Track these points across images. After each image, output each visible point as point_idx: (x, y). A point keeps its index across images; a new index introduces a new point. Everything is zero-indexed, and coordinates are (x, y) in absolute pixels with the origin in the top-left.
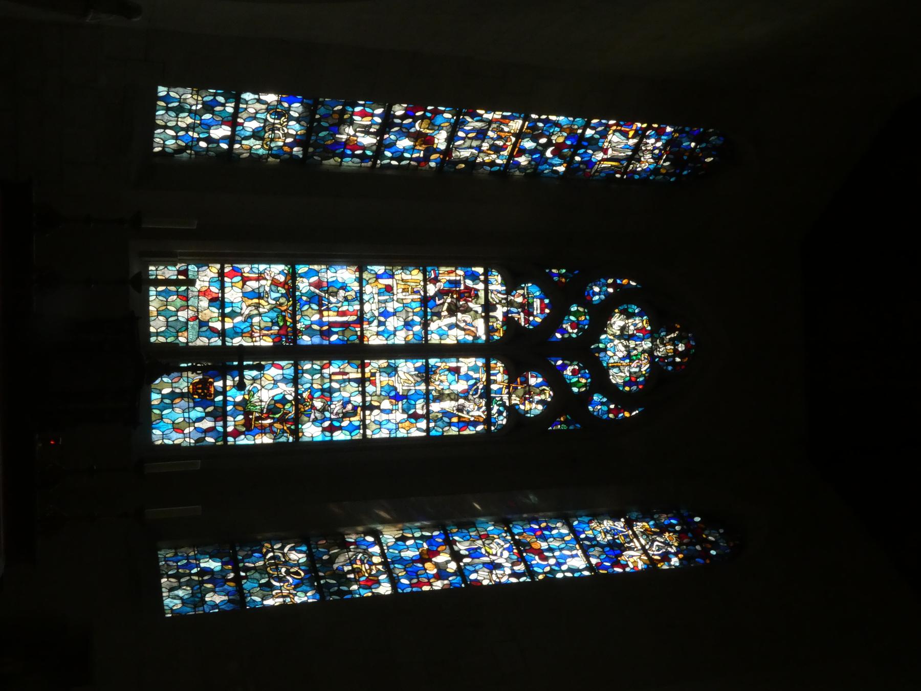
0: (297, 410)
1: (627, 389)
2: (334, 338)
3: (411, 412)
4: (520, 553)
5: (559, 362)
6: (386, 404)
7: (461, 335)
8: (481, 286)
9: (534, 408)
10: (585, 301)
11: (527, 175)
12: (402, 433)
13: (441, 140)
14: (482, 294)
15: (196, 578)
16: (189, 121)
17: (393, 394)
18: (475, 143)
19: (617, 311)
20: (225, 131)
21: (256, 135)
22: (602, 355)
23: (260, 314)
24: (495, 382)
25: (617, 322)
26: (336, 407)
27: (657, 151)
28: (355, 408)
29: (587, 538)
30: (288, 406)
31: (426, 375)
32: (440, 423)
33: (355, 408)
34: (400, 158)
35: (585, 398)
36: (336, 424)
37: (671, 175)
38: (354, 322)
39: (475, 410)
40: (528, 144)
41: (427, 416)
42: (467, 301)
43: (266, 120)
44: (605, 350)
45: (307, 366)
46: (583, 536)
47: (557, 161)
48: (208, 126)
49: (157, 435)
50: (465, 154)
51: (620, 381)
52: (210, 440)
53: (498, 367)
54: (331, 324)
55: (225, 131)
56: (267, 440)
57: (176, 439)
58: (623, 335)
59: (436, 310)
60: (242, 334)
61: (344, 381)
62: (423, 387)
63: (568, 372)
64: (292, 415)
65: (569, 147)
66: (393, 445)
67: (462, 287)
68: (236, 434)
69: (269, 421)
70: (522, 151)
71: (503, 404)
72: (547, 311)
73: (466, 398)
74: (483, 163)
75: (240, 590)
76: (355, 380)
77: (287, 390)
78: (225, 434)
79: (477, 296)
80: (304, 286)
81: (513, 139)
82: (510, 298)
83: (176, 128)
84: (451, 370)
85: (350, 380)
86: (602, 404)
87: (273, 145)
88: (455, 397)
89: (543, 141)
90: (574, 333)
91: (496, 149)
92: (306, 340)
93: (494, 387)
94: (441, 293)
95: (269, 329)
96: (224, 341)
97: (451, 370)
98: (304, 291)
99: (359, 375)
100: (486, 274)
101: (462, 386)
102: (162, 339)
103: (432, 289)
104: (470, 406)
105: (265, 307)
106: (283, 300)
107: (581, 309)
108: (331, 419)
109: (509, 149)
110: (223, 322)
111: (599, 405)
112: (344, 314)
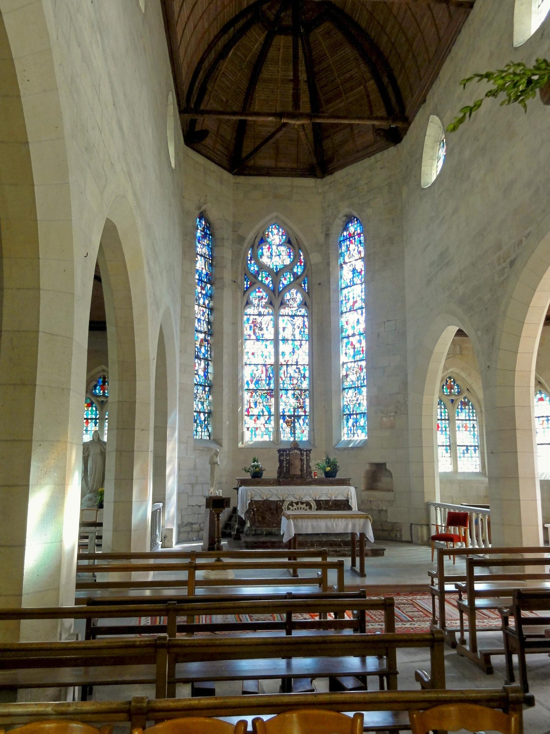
0: (297, 390)
1: (292, 257)
2: (271, 375)
3: (299, 347)
4: (354, 310)
5: (281, 286)
6: (295, 357)
8: (252, 317)
9: (299, 297)
10: (258, 273)
11: (211, 300)
12: (307, 351)
13: (202, 336)
14: (255, 317)
15: (355, 428)
16: (199, 427)
17: (292, 354)
18: (202, 322)
19: (261, 260)
20: (202, 415)
21: (203, 404)
22: (278, 267)
23: (263, 402)
24: (288, 313)
25: (265, 260)
26: (296, 375)
27: (202, 247)
28: (297, 368)
29: (350, 282)
30: (296, 393)
31: (285, 340)
32: (303, 336)
33: (297, 368)
34: (208, 351)
35: (294, 274)
36: (303, 375)
37: (209, 238)
38: (266, 368)
39: (298, 321)
40: (201, 301)
42: (257, 323)
43: (198, 401)
44: (276, 266)
45: (282, 385)
46: (349, 284)
47: (206, 288)
48: (201, 421)
50: (205, 325)
51: (289, 260)
52: (307, 421)
53: (283, 311)
54: (266, 376)
55: (202, 415)
56: (307, 401)
57: (306, 433)
58: (271, 257)
59: (261, 336)
60: (270, 409)
61: (287, 372)
62: (290, 342)
64: (299, 392)
65: (202, 283)
66: (311, 354)
67: (252, 325)
68: (305, 412)
69: (301, 399)
70: (204, 303)
71: (297, 310)
72: (261, 290)
73: (294, 325)
74: (208, 318)
75: (360, 414)
76: (287, 368)
77: (290, 393)
78: (305, 415)
79: (255, 319)
80: (252, 386)
81: (200, 307)
82: (256, 305)
83: (202, 432)
84: (284, 331)
85: (287, 370)
86: (297, 268)
87: (205, 398)
88: (294, 328)
89: (200, 295)
90: (270, 279)
92: (272, 386)
93: (290, 314)
94: (254, 333)
95: (268, 399)
96: (273, 415)
97: (284, 331)
98: (254, 386)
99: (285, 366)
100: (247, 315)
101: (289, 327)
102: (271, 437)
103: (253, 337)
105: (260, 400)
106: (257, 394)
107: (260, 275)
108: (301, 377)
109: (203, 309)
110: (265, 415)
111: (298, 270)
112: (262, 373)
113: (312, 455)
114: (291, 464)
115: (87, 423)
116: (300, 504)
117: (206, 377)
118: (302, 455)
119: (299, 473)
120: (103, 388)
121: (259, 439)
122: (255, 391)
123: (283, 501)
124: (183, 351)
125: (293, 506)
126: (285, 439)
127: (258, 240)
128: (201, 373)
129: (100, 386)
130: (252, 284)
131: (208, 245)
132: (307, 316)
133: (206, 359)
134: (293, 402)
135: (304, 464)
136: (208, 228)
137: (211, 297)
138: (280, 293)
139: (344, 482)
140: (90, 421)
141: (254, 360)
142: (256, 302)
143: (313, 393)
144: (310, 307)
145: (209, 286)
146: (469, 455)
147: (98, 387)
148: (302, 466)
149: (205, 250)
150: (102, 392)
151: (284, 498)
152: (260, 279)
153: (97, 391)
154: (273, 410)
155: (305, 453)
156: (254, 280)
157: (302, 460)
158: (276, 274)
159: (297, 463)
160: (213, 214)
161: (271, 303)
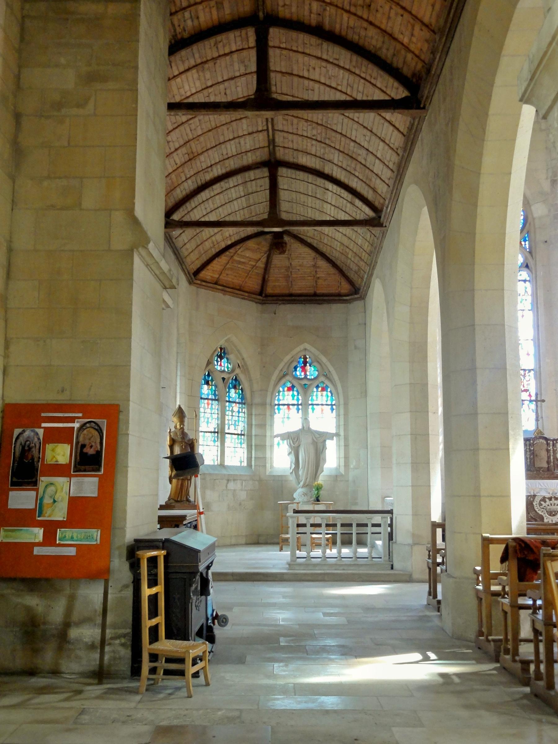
114: (536, 456)
115: (289, 408)
116: (553, 499)
118: (548, 444)
119: (545, 465)
120: (304, 369)
123: (534, 496)
125: (545, 502)
129: (302, 367)
132: (529, 281)
135: (550, 455)
140: (291, 407)
143: (540, 374)
144: (534, 272)
147: (298, 369)
148: (549, 457)
150: (303, 374)
151: (535, 493)
153: (298, 373)
155: (551, 443)
157: (548, 451)
159: (544, 454)
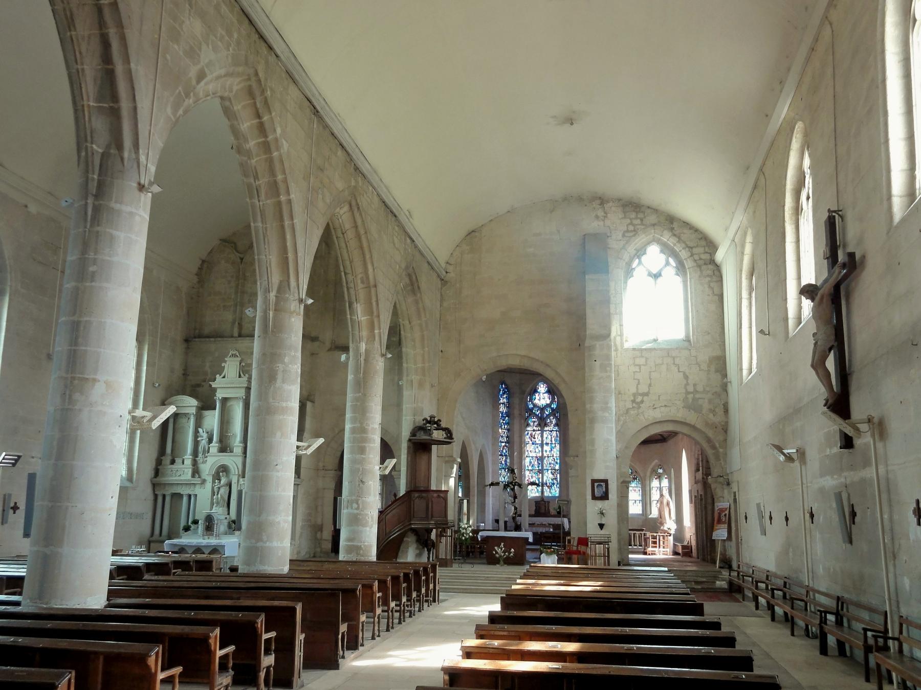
6: (552, 452)
7: (539, 436)
8: (530, 432)
9: (554, 421)
10: (533, 409)
12: (558, 449)
13: (503, 444)
21: (504, 478)
25: (536, 401)
26: (553, 462)
31: (547, 444)
35: (552, 409)
40: (503, 427)
41: (555, 444)
49: (557, 495)
50: (505, 438)
52: (558, 486)
53: (546, 429)
56: (558, 475)
57: (558, 492)
62: (549, 445)
63: (547, 413)
70: (504, 428)
77: (550, 471)
80: (530, 468)
88: (552, 438)
90: (539, 411)
91: (504, 433)
92: (540, 468)
94: (531, 440)
101: (549, 437)
103: (531, 442)
104: (553, 435)
105: (534, 475)
111: (554, 406)
113: (550, 505)
117: (506, 464)
121: (535, 495)
122: (532, 470)
124: (493, 454)
126: (547, 495)
127: (532, 392)
128: (503, 462)
130: (530, 415)
131: (506, 397)
133: (506, 456)
134: (551, 476)
136: (506, 388)
137: (508, 424)
138: (544, 419)
139: (564, 516)
141: (531, 455)
142: (532, 424)
145: (507, 418)
146: (636, 505)
149: (505, 400)
152: (534, 411)
154: (540, 480)
156: (530, 413)
157: (545, 506)
158: (542, 409)
160: (508, 381)
161: (539, 425)
